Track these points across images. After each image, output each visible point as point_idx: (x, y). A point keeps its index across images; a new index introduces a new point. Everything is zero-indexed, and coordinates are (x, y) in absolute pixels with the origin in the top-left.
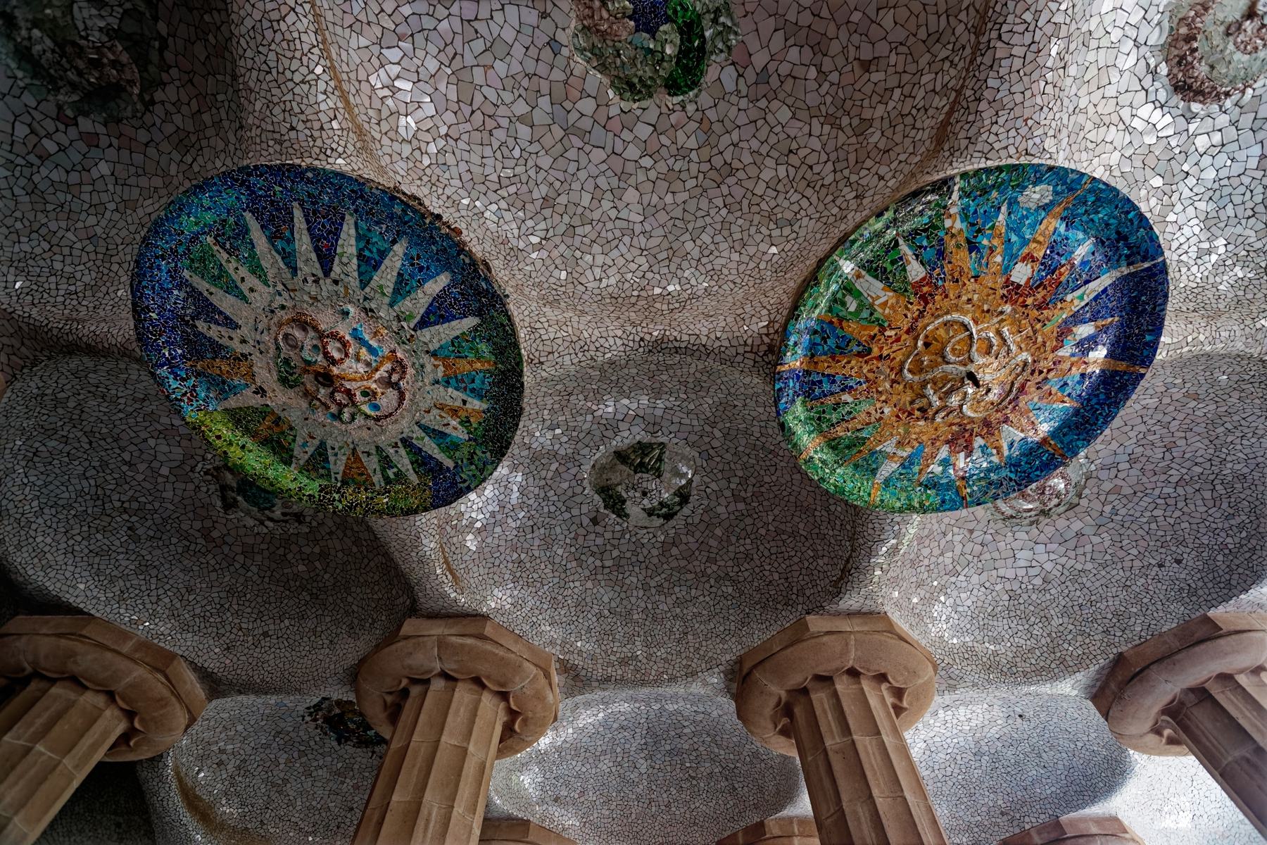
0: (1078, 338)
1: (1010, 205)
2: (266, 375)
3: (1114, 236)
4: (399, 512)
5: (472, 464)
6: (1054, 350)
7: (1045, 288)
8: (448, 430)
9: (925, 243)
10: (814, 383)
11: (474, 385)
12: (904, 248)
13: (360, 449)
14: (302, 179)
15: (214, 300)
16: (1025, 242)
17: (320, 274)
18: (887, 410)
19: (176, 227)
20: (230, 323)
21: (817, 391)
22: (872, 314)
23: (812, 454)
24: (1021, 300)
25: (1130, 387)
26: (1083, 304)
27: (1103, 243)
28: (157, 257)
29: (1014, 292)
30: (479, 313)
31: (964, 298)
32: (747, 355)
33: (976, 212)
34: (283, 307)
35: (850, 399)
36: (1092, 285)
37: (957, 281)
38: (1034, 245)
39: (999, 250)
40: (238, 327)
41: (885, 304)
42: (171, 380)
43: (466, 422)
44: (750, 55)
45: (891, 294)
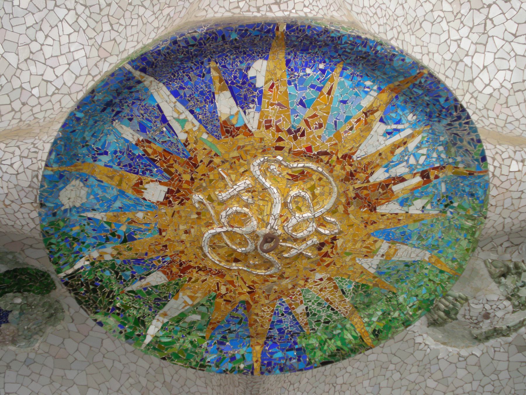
0: (236, 109)
1: (85, 210)
3: (109, 110)
6: (250, 133)
7: (171, 166)
9: (129, 273)
12: (136, 286)
16: (122, 193)
18: (318, 276)
22: (203, 305)
23: (370, 330)
24: (185, 186)
25: (309, 33)
26: (191, 117)
27: (118, 112)
29: (176, 195)
31: (184, 237)
33: (95, 238)
35: (303, 307)
36: (168, 113)
37: (166, 246)
38: (124, 184)
39: (131, 216)
41: (191, 297)
44: (13, 241)
45: (181, 294)
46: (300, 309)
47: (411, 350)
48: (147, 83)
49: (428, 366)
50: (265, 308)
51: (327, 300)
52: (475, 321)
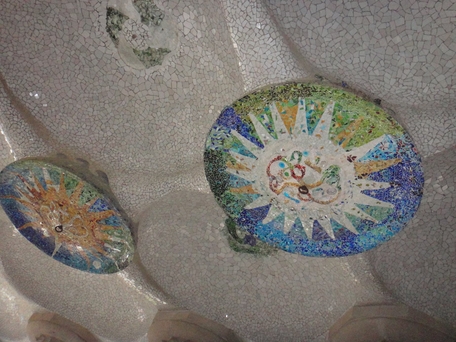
2: (348, 171)
3: (69, 257)
4: (252, 97)
5: (221, 138)
8: (240, 156)
10: (104, 206)
11: (237, 181)
13: (287, 134)
14: (328, 253)
15: (376, 200)
17: (319, 221)
18: (71, 203)
19: (389, 230)
20: (368, 193)
21: (100, 203)
28: (402, 218)
30: (245, 212)
32: (135, 205)
34: (337, 205)
40: (363, 192)
41: (107, 236)
42: (410, 155)
43: (233, 162)
46: (89, 204)
47: (185, 57)
48: (57, 250)
49: (191, 41)
50: (96, 215)
51: (79, 197)
52: (143, 38)
